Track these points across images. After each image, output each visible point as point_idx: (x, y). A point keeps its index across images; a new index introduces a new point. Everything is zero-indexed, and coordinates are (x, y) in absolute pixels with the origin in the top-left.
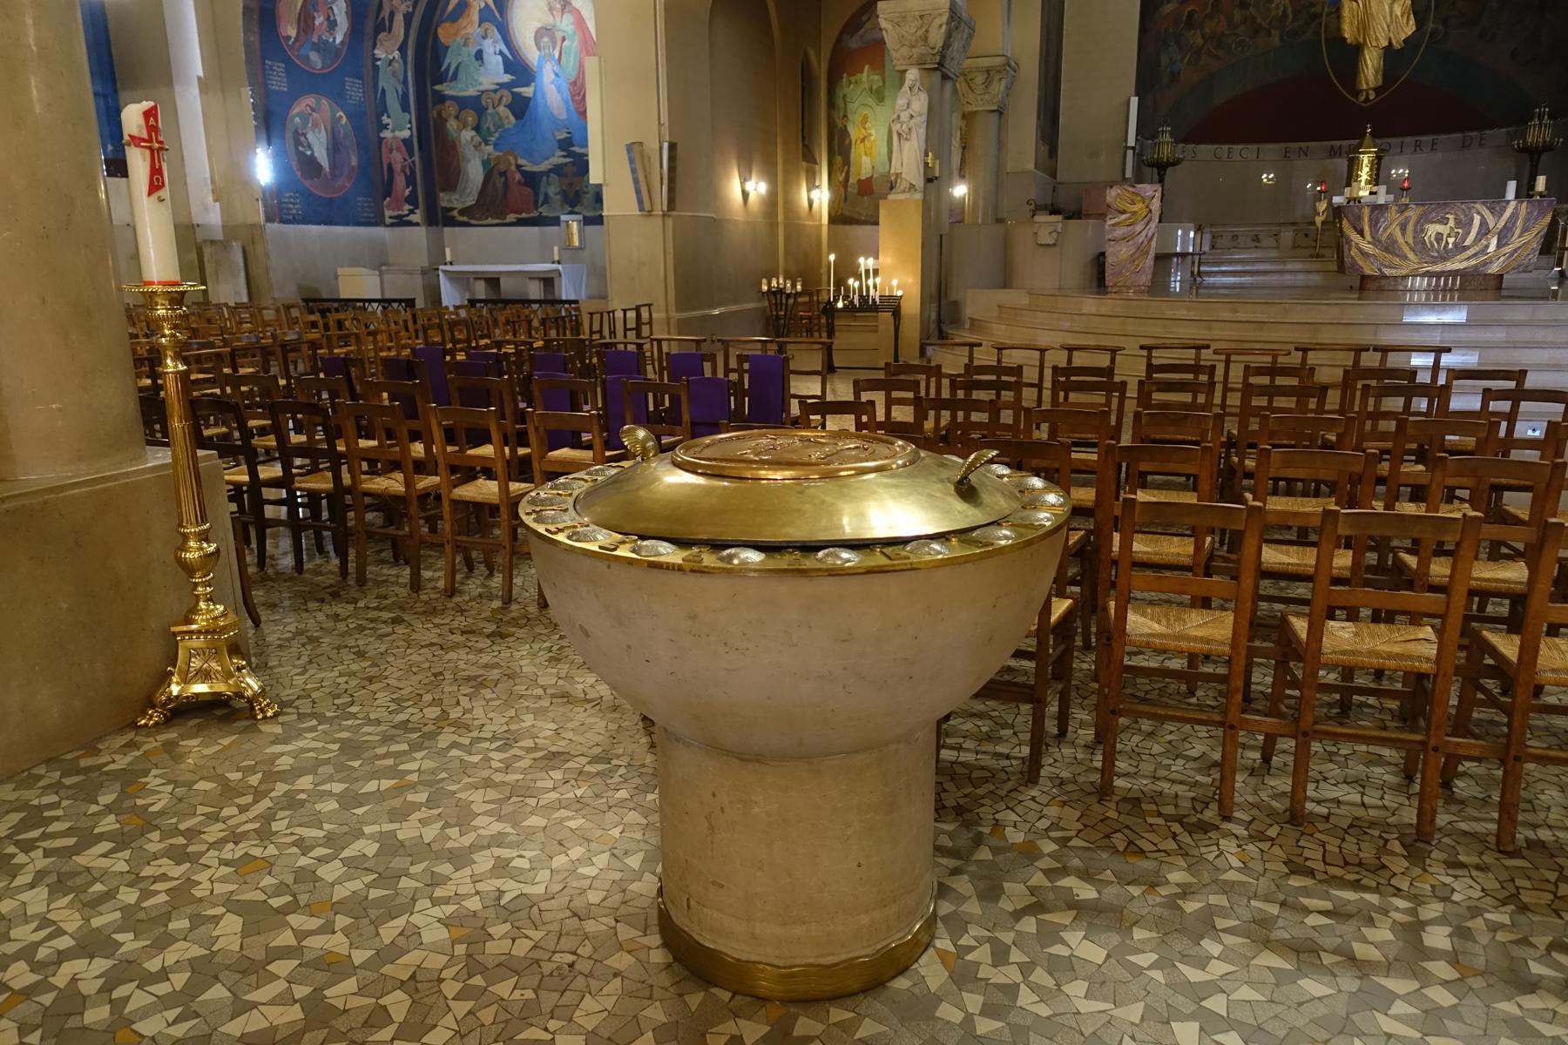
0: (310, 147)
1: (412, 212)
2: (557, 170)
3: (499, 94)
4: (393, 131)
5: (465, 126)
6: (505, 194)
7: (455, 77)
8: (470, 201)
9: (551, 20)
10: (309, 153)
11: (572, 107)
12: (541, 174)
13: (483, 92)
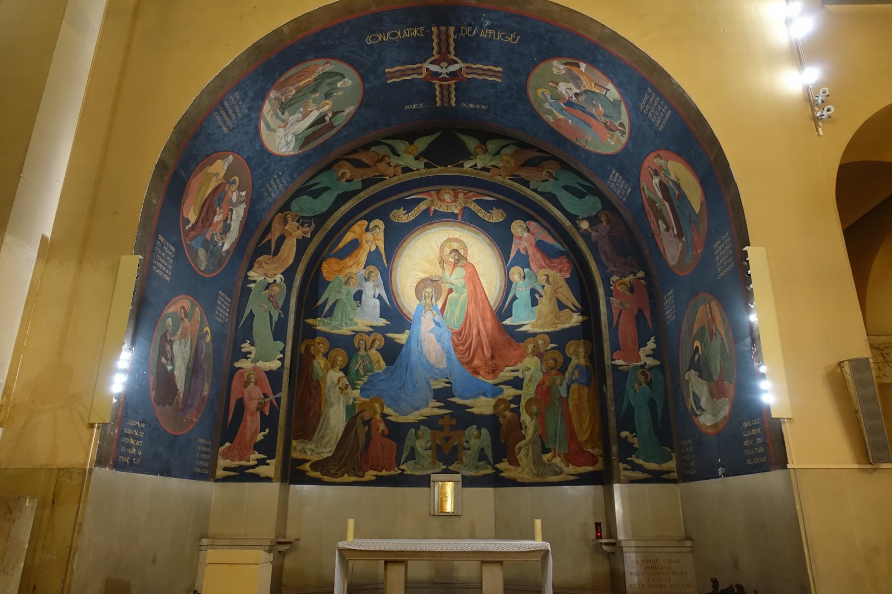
0: (172, 361)
1: (262, 462)
2: (430, 422)
3: (372, 337)
4: (255, 361)
5: (333, 367)
6: (367, 446)
7: (330, 313)
8: (327, 452)
9: (439, 272)
10: (170, 368)
11: (454, 357)
12: (409, 425)
13: (357, 332)
